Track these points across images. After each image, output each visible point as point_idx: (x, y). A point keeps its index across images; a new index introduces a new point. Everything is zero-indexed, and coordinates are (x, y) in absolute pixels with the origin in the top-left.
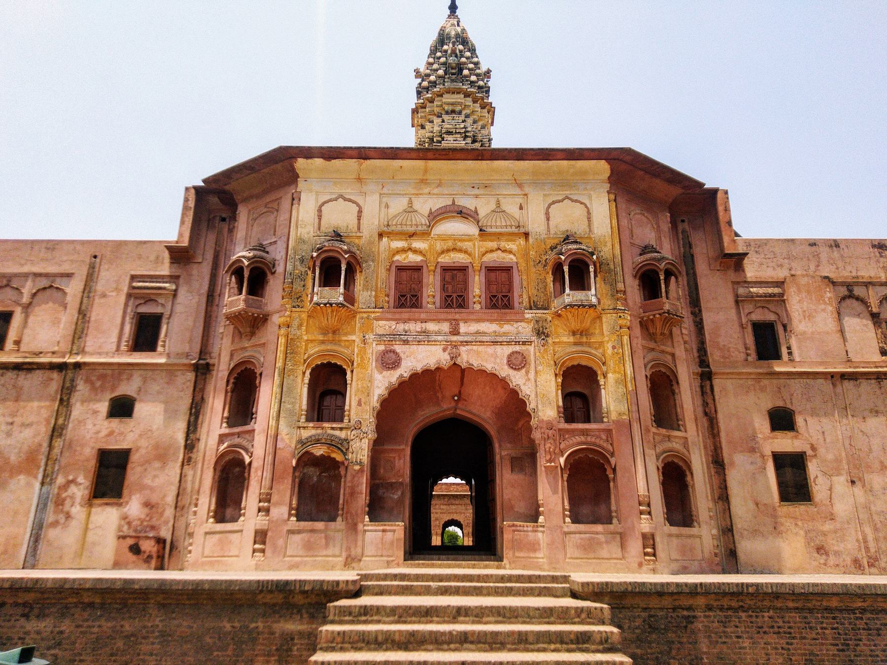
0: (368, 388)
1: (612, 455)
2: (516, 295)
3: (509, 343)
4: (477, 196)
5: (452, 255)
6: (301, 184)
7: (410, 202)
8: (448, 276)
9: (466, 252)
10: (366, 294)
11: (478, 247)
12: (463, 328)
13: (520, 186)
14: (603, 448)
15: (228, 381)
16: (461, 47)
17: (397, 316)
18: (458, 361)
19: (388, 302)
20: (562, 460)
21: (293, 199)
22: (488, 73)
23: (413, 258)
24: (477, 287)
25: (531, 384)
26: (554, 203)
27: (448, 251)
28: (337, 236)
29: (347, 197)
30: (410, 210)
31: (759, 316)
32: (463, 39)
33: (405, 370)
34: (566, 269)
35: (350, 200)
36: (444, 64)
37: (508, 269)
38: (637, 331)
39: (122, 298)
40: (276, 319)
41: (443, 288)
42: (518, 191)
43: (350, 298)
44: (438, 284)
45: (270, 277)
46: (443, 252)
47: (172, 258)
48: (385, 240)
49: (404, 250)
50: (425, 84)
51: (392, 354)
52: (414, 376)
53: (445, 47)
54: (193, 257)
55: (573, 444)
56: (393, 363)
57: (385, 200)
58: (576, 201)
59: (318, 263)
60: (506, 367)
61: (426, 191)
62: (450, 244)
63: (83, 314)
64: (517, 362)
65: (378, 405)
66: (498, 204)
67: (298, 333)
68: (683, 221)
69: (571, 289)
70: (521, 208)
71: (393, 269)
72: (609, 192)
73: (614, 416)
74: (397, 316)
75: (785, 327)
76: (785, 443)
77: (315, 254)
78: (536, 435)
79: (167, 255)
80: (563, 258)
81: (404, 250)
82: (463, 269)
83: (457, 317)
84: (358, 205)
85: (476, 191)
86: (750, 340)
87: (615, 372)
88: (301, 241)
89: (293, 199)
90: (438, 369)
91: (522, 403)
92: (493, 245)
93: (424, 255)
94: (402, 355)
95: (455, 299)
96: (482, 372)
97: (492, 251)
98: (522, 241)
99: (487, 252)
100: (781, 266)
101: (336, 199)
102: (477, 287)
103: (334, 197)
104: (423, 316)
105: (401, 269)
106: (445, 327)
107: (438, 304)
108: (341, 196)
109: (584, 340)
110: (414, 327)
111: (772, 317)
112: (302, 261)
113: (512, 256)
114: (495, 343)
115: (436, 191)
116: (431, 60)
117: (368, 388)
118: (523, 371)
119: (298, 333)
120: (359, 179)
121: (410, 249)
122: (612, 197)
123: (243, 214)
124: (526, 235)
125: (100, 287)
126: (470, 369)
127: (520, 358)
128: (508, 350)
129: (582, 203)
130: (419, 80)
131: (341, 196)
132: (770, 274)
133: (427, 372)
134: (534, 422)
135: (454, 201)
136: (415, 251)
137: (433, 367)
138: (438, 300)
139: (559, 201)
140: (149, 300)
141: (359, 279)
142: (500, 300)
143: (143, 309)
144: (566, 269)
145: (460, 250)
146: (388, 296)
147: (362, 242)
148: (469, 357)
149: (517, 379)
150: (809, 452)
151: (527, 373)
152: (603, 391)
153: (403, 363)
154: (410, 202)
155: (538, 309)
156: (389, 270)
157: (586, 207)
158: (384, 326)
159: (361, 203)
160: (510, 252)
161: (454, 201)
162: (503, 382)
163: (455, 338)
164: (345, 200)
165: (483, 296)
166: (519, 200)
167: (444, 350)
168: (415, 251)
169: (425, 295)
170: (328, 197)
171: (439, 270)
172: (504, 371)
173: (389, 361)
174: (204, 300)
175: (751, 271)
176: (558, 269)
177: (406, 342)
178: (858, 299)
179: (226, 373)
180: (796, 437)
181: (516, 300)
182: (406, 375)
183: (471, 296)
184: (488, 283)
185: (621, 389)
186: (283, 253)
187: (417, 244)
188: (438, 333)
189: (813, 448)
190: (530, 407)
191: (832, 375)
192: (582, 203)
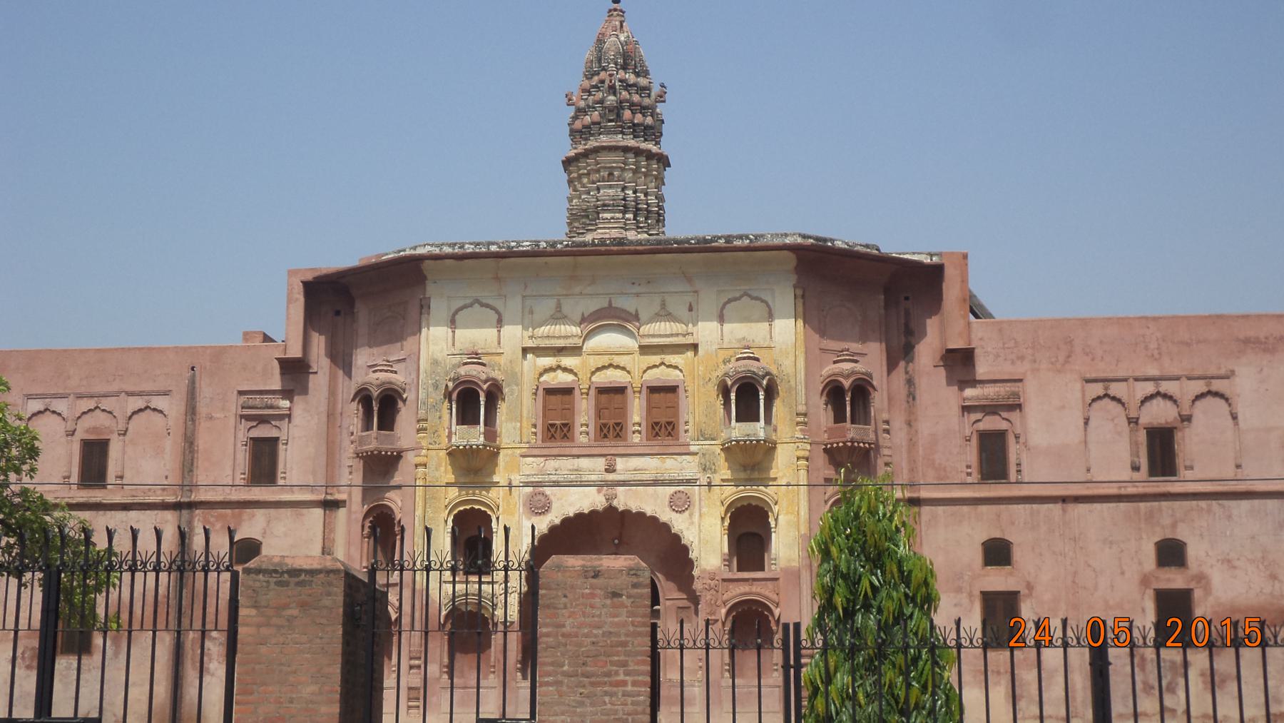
0: (516, 531)
1: (777, 605)
2: (682, 421)
3: (670, 483)
4: (637, 295)
5: (610, 372)
6: (431, 289)
7: (559, 306)
8: (604, 397)
9: (623, 369)
10: (510, 425)
11: (637, 363)
12: (620, 463)
13: (689, 280)
14: (767, 598)
15: (363, 526)
16: (621, 74)
17: (546, 452)
18: (615, 503)
19: (535, 434)
20: (724, 611)
21: (422, 307)
22: (661, 98)
23: (562, 379)
24: (637, 411)
25: (695, 530)
26: (729, 301)
27: (604, 367)
28: (475, 357)
29: (484, 301)
30: (559, 315)
31: (991, 423)
32: (628, 59)
33: (554, 517)
34: (733, 396)
35: (487, 306)
36: (601, 102)
37: (672, 389)
38: (821, 459)
39: (232, 421)
40: (410, 458)
41: (599, 414)
42: (688, 288)
43: (491, 435)
44: (592, 412)
45: (400, 404)
46: (598, 369)
47: (281, 368)
48: (530, 356)
49: (551, 369)
50: (578, 125)
51: (540, 497)
52: (567, 522)
53: (603, 75)
54: (309, 367)
55: (737, 593)
56: (543, 507)
57: (528, 302)
58: (757, 298)
59: (454, 396)
60: (668, 509)
61: (577, 290)
62: (605, 360)
63: (189, 442)
64: (680, 504)
65: (527, 557)
66: (663, 305)
67: (437, 474)
68: (907, 298)
69: (737, 421)
70: (691, 309)
71: (541, 392)
72: (795, 287)
73: (782, 563)
74: (546, 452)
75: (1017, 437)
76: (998, 580)
77: (451, 385)
78: (697, 585)
79: (276, 363)
80: (729, 383)
81: (551, 369)
82: (621, 390)
83: (613, 451)
84: (497, 312)
85: (636, 289)
86: (971, 455)
87: (787, 513)
88: (435, 363)
89: (422, 307)
90: (593, 512)
91: (685, 550)
92: (656, 359)
93: (576, 374)
94: (552, 498)
95: (611, 429)
96: (641, 515)
97: (655, 366)
98: (690, 354)
99: (649, 368)
100: (1022, 358)
101: (471, 305)
102: (637, 411)
103: (468, 301)
104: (575, 451)
105: (550, 392)
106: (600, 463)
107: (592, 435)
108: (477, 301)
109: (756, 475)
110: (566, 465)
111: (1003, 425)
112: (436, 387)
113: (678, 372)
114: (656, 483)
115: (589, 290)
116: (587, 84)
117: (516, 531)
118: (687, 513)
119: (437, 474)
120: (497, 279)
121: (559, 367)
122: (799, 292)
123: (363, 313)
124: (695, 347)
125: (202, 409)
126: (627, 513)
127: (683, 497)
128: (671, 490)
129: (763, 301)
130: (571, 111)
131: (477, 301)
132: (1007, 370)
133: (579, 516)
134: (696, 572)
135: (610, 302)
136: (565, 370)
137: (586, 511)
138: (592, 429)
139: (735, 299)
140: (263, 420)
141: (503, 409)
142: (664, 429)
143: (256, 433)
144: (733, 396)
145: (617, 367)
146: (535, 426)
147: (502, 360)
148: (627, 500)
149: (679, 524)
150: (1024, 591)
151: (691, 515)
152: (773, 535)
153: (554, 506)
154: (559, 307)
155: (706, 439)
156: (535, 394)
157: (768, 306)
158: (531, 467)
159: (501, 309)
160: (676, 367)
161: (610, 302)
162: (666, 527)
163: (611, 477)
164: (482, 305)
165: (644, 424)
166: (689, 298)
167: (599, 492)
168: (565, 370)
169: (577, 424)
170: (460, 303)
171: (592, 392)
172: (665, 515)
173: (539, 506)
174: (324, 419)
175: (983, 369)
176: (725, 391)
177: (556, 484)
178: (1114, 398)
179: (361, 517)
180: (1011, 574)
181: (682, 428)
182: (557, 521)
183: (630, 424)
184: (650, 408)
185: (794, 533)
186: (414, 376)
187: (567, 361)
188: (592, 471)
189: (1030, 587)
190: (692, 555)
191: (1064, 500)
192: (763, 301)
